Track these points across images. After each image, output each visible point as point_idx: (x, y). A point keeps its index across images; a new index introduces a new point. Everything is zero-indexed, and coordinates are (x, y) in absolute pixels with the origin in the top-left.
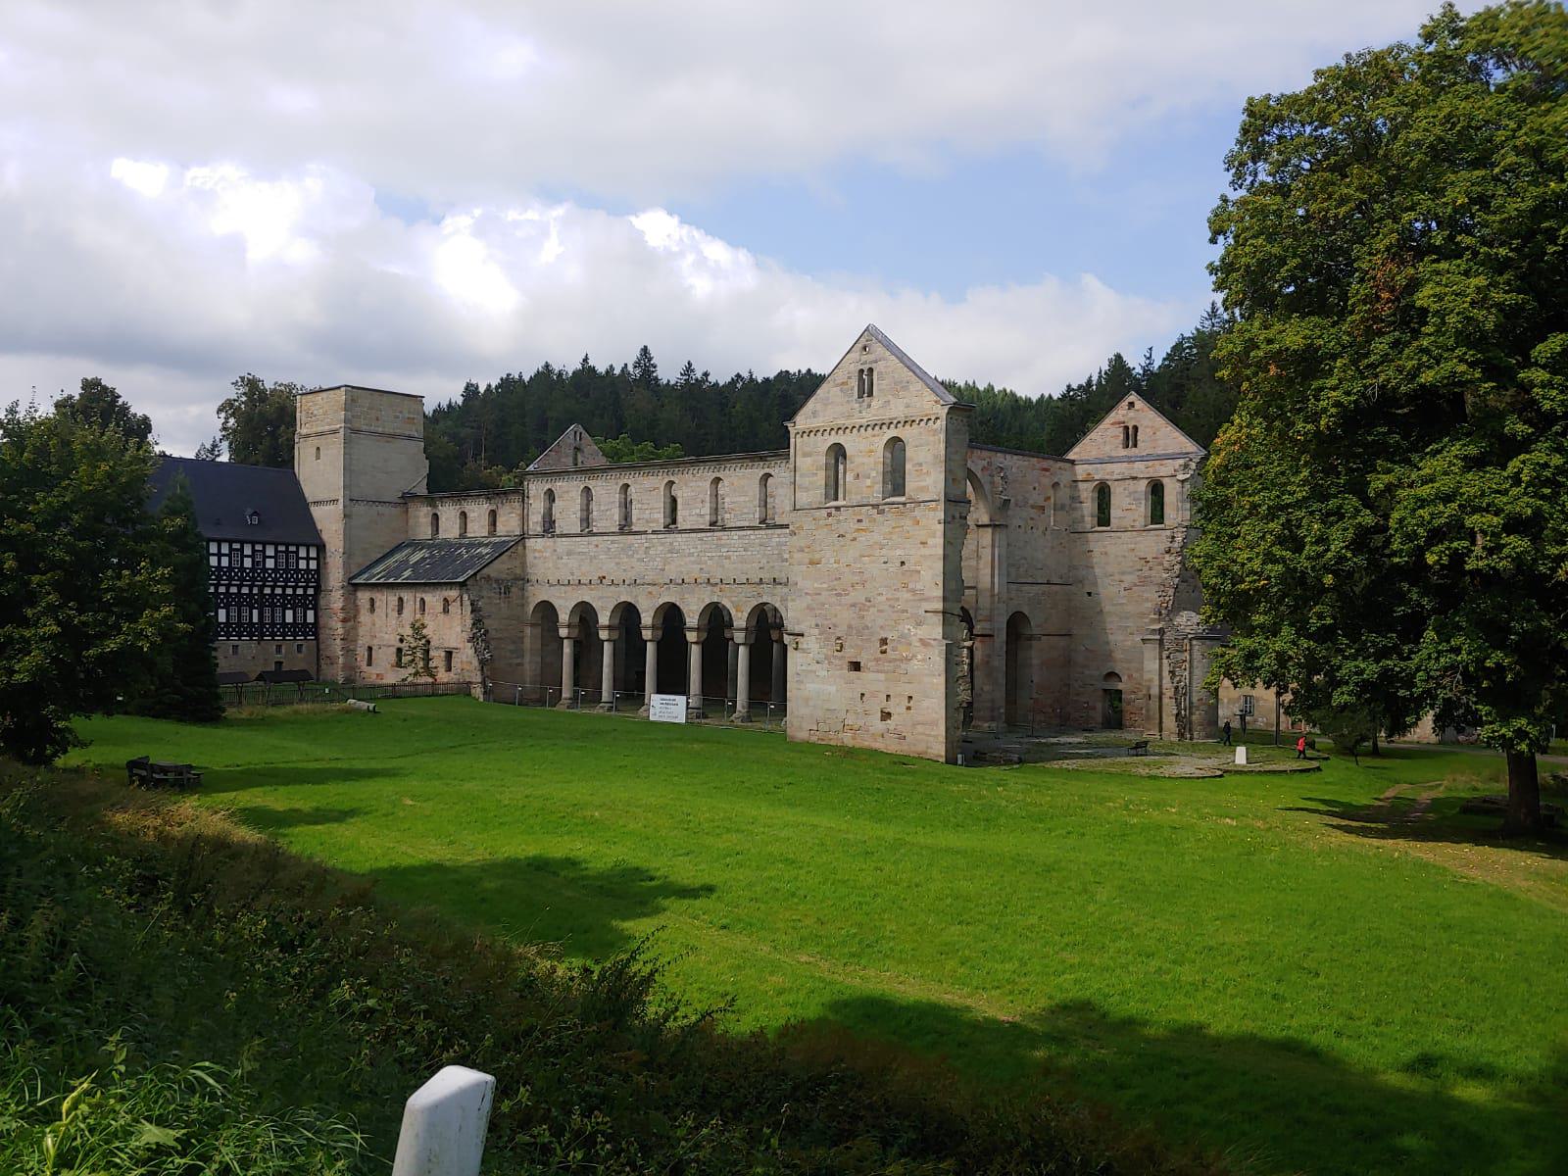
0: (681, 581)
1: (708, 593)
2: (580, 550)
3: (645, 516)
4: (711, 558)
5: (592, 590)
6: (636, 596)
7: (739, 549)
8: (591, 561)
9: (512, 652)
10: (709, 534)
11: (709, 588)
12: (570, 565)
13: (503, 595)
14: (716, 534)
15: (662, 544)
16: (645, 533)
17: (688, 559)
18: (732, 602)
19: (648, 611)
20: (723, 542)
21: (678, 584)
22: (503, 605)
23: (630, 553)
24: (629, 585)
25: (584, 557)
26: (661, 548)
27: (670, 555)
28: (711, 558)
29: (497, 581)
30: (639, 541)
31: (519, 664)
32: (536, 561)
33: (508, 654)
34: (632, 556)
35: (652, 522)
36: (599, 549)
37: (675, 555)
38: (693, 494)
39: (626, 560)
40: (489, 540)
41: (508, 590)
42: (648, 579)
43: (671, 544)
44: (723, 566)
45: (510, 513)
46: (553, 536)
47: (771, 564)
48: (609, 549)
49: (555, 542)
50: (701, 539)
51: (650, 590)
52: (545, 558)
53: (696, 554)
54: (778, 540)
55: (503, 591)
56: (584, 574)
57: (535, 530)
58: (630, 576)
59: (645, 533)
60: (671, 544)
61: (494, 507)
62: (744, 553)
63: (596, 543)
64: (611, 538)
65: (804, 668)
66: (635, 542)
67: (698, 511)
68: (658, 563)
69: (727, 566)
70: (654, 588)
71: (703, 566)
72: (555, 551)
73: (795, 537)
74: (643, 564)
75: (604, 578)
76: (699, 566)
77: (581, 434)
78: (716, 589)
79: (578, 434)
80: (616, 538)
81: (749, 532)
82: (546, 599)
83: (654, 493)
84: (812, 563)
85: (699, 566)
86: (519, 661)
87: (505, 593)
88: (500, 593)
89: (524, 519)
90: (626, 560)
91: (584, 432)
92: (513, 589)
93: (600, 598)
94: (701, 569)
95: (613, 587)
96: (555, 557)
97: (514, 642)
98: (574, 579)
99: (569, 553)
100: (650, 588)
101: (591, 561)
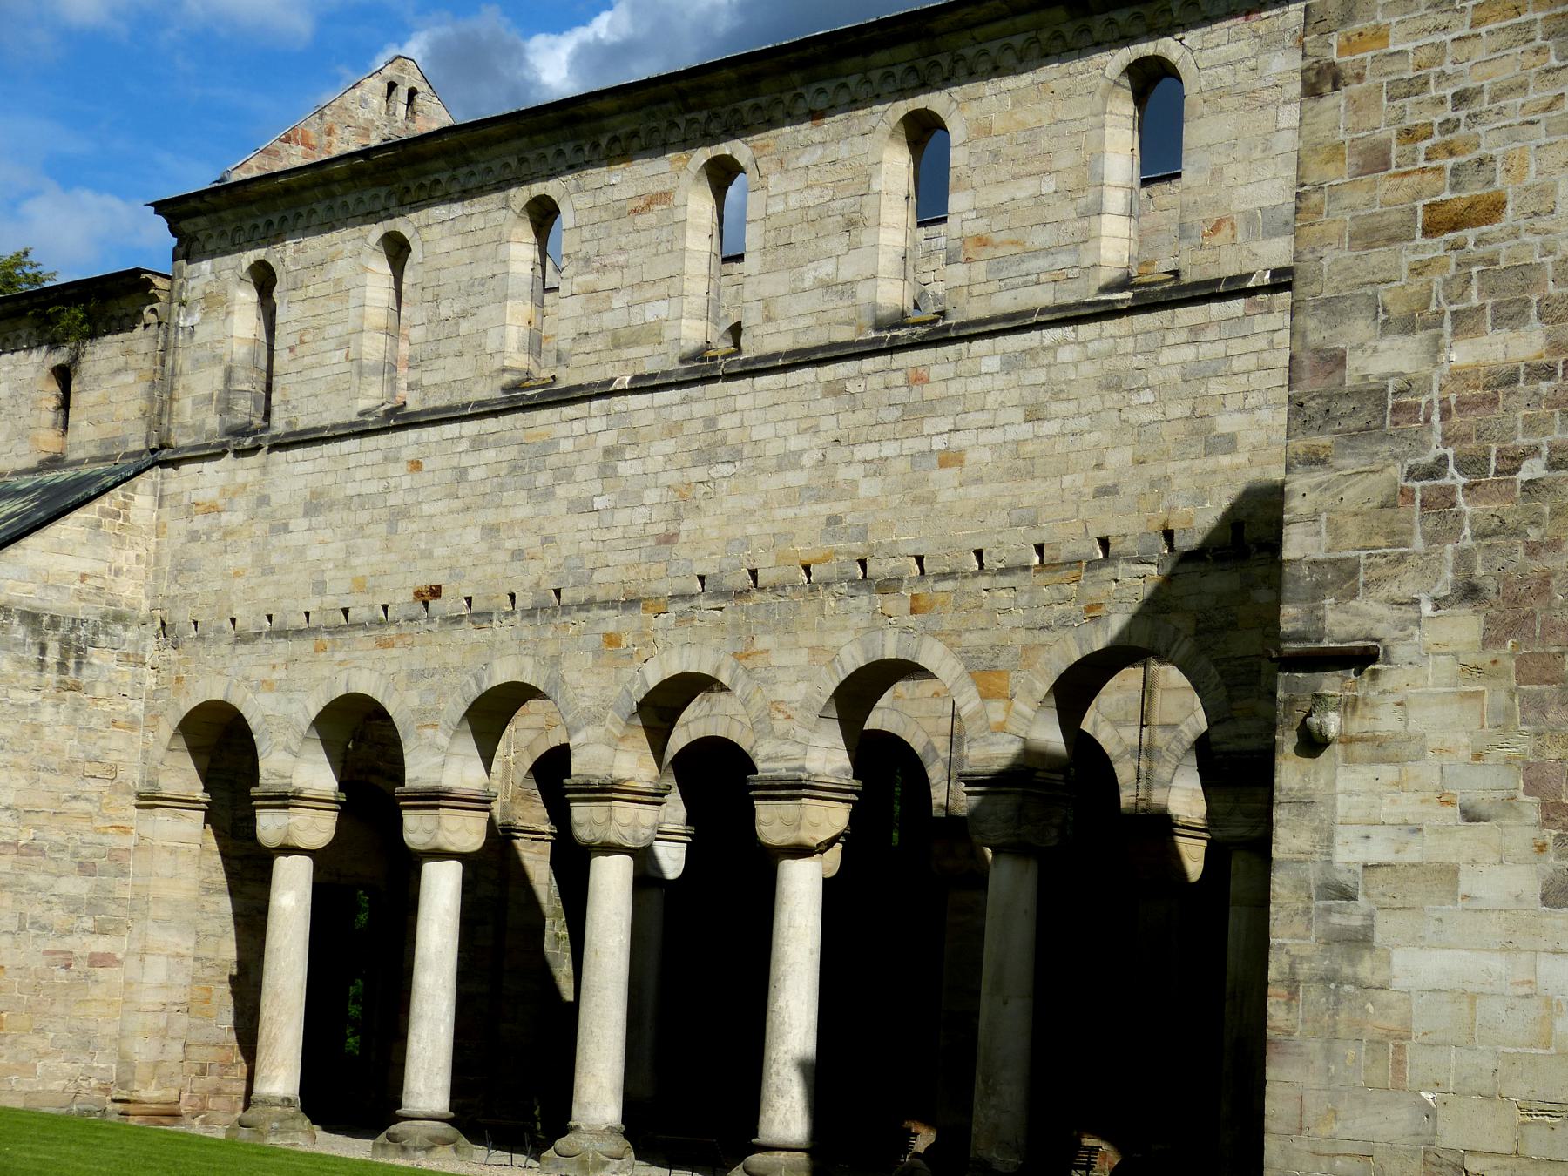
0: (744, 580)
1: (860, 621)
2: (351, 489)
3: (609, 320)
4: (877, 468)
5: (384, 644)
6: (555, 660)
7: (1003, 417)
8: (392, 530)
9: (74, 905)
10: (868, 364)
11: (863, 600)
12: (313, 553)
13: (51, 676)
14: (902, 359)
15: (673, 430)
16: (604, 391)
17: (774, 482)
18: (966, 656)
19: (596, 719)
20: (930, 392)
21: (726, 594)
22: (47, 714)
23: (543, 479)
24: (530, 614)
25: (364, 516)
26: (669, 446)
27: (699, 473)
28: (877, 468)
29: (31, 618)
30: (578, 427)
31: (101, 960)
32: (196, 549)
33: (58, 916)
34: (548, 493)
35: (637, 343)
36: (424, 478)
37: (726, 469)
38: (811, 198)
39: (523, 511)
40: (38, 478)
41: (75, 653)
42: (608, 581)
43: (710, 423)
44: (930, 500)
45: (117, 372)
46: (255, 450)
47: (1153, 470)
48: (462, 473)
49: (264, 468)
50: (835, 390)
51: (611, 627)
52: (228, 533)
53: (807, 460)
54: (1188, 353)
55: (52, 657)
56: (360, 586)
57: (198, 429)
58: (529, 580)
59: (604, 391)
60: (710, 423)
61: (60, 357)
62: (1027, 430)
63: (409, 453)
64: (471, 427)
65: (1378, 851)
66: (563, 430)
67: (826, 269)
68: (649, 515)
69: (945, 496)
70: (625, 617)
71: (838, 508)
72: (264, 500)
73: (1340, 97)
74: (587, 521)
75: (436, 592)
76: (824, 509)
77: (412, 93)
78: (897, 604)
79: (402, 95)
80: (490, 424)
81: (1051, 335)
82: (218, 695)
83: (650, 218)
84: (1440, 222)
85: (824, 509)
86: (101, 945)
87: (62, 666)
88: (42, 664)
89: (163, 384)
90: (523, 511)
91: (422, 88)
92: (96, 657)
93: (415, 676)
94: (833, 520)
95: (467, 634)
96: (260, 528)
97: (85, 869)
98: (323, 606)
99: (315, 505)
100: (612, 621)
101: (392, 530)
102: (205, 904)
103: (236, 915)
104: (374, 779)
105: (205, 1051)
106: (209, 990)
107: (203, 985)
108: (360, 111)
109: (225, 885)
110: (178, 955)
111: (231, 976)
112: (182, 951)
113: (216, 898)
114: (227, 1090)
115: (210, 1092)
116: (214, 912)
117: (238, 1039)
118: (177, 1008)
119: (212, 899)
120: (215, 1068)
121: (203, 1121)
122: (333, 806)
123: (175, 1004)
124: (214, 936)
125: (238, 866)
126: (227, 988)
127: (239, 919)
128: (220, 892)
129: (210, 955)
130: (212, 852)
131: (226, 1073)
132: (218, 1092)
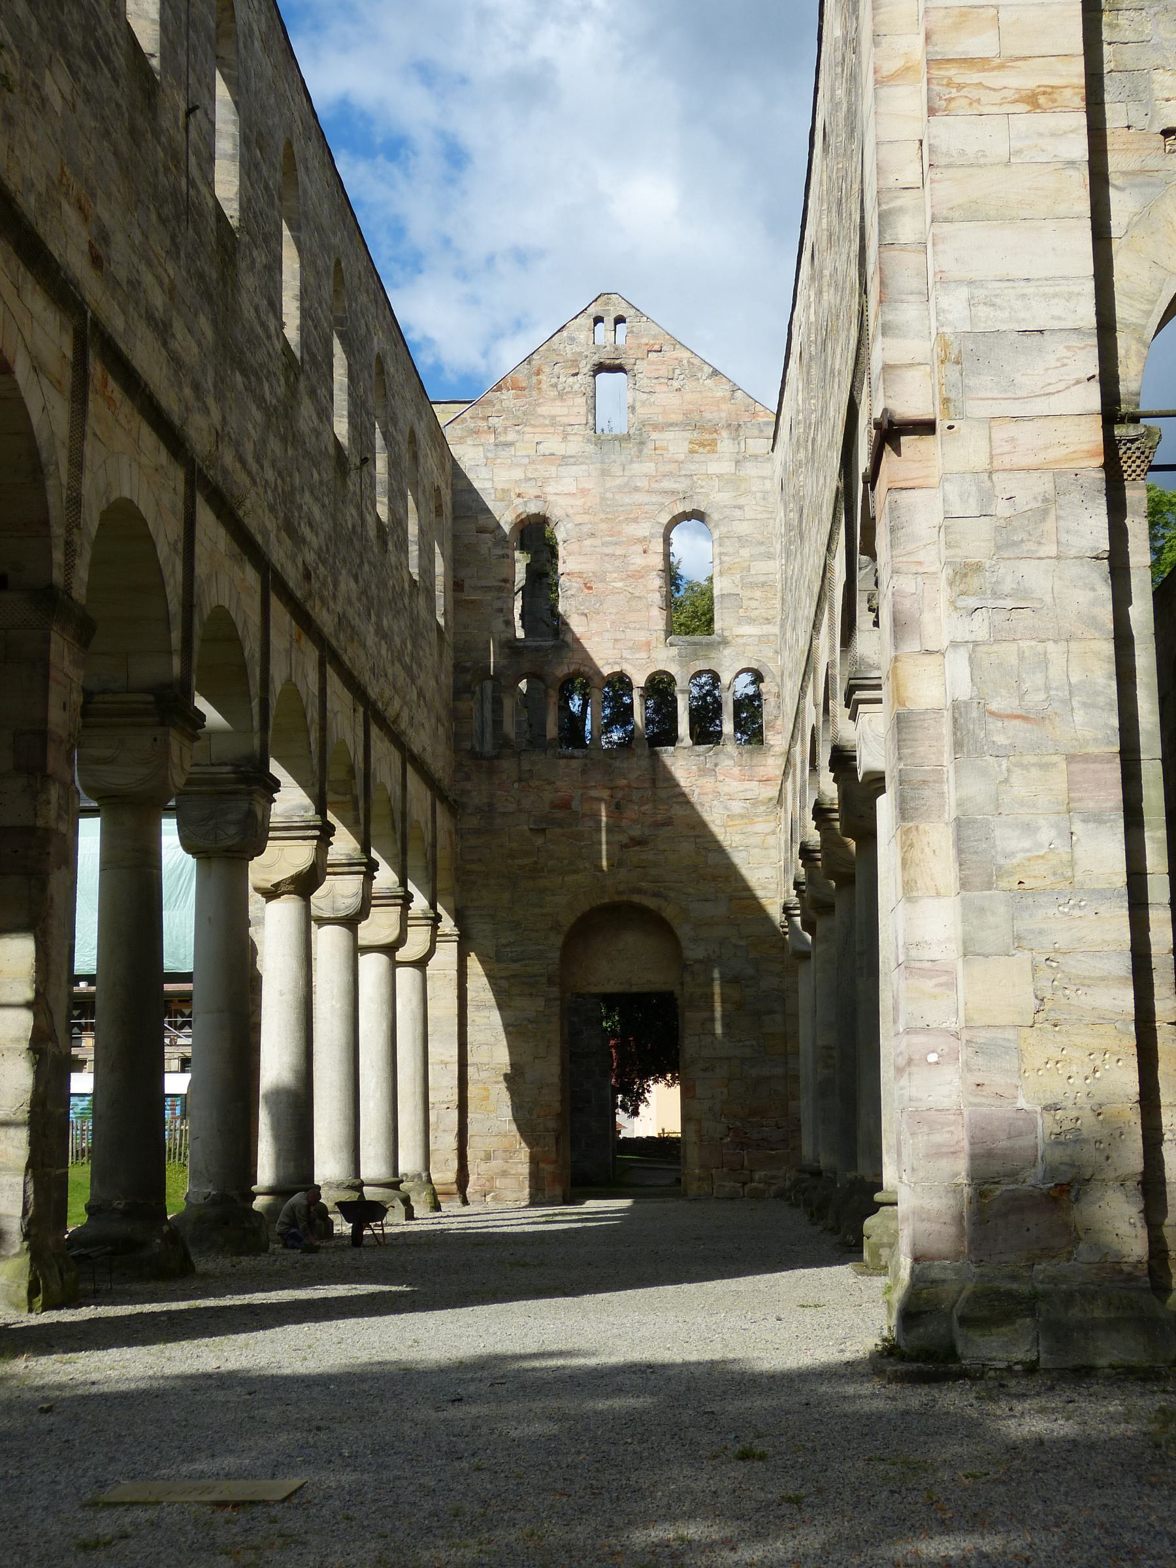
102: (475, 1018)
103: (506, 1026)
104: (636, 898)
105: (488, 1140)
106: (486, 1089)
107: (481, 1086)
108: (568, 348)
109: (493, 1002)
110: (442, 1062)
111: (506, 1075)
112: (445, 1058)
113: (486, 1013)
114: (513, 1172)
115: (496, 1174)
116: (485, 1025)
117: (519, 1129)
118: (446, 1106)
119: (483, 1014)
120: (499, 1153)
121: (494, 1198)
122: (424, 922)
123: (443, 1102)
124: (487, 1044)
125: (504, 984)
126: (503, 1085)
127: (510, 1029)
128: (491, 1007)
129: (485, 1060)
130: (478, 975)
131: (511, 1158)
132: (504, 1174)
